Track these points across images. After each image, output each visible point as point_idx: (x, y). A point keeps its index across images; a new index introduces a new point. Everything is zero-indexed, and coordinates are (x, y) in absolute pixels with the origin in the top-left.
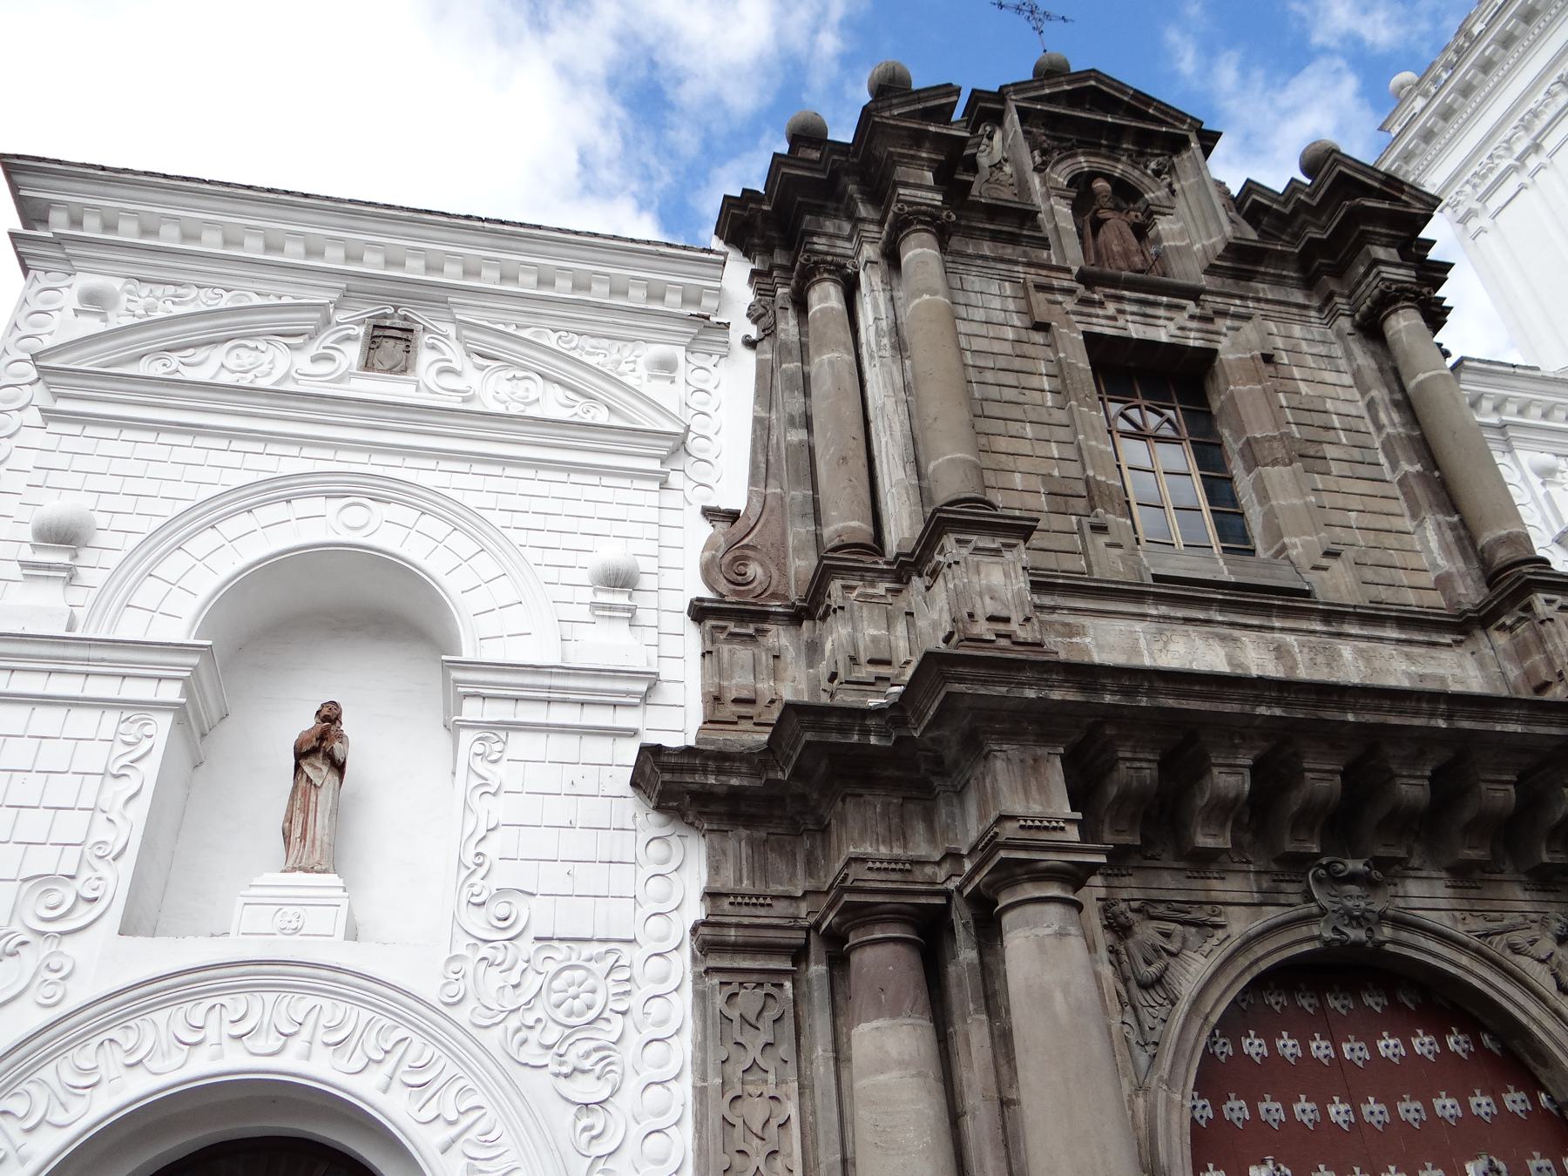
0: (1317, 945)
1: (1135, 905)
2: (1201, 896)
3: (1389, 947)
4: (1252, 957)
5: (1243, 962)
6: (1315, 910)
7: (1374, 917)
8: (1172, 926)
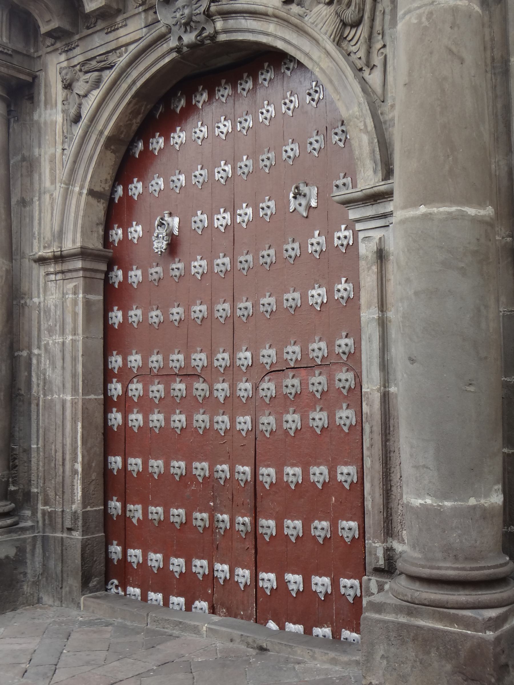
0: (174, 55)
1: (78, 67)
2: (113, 45)
3: (222, 38)
4: (129, 80)
5: (124, 86)
6: (164, 30)
7: (202, 18)
8: (90, 74)
